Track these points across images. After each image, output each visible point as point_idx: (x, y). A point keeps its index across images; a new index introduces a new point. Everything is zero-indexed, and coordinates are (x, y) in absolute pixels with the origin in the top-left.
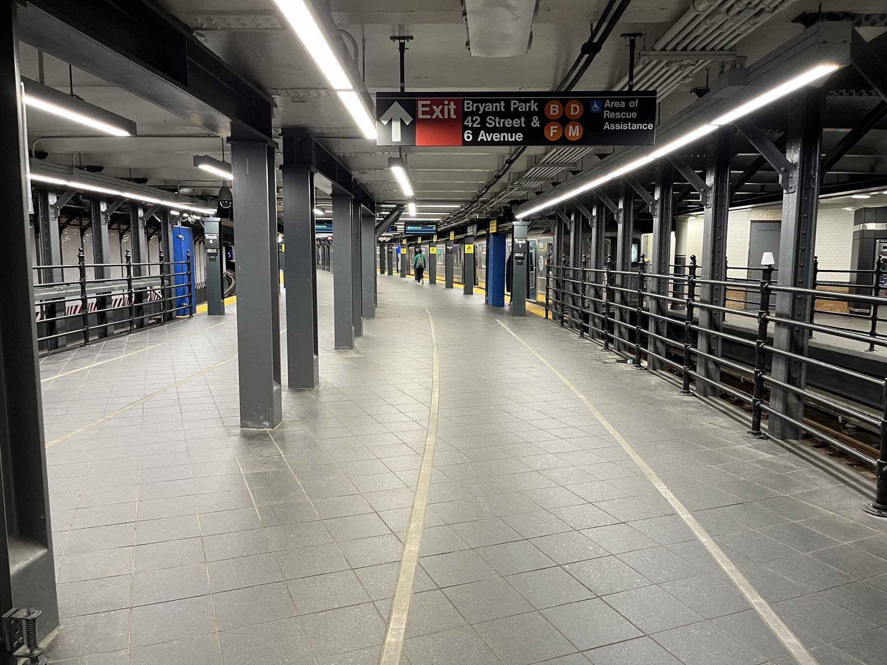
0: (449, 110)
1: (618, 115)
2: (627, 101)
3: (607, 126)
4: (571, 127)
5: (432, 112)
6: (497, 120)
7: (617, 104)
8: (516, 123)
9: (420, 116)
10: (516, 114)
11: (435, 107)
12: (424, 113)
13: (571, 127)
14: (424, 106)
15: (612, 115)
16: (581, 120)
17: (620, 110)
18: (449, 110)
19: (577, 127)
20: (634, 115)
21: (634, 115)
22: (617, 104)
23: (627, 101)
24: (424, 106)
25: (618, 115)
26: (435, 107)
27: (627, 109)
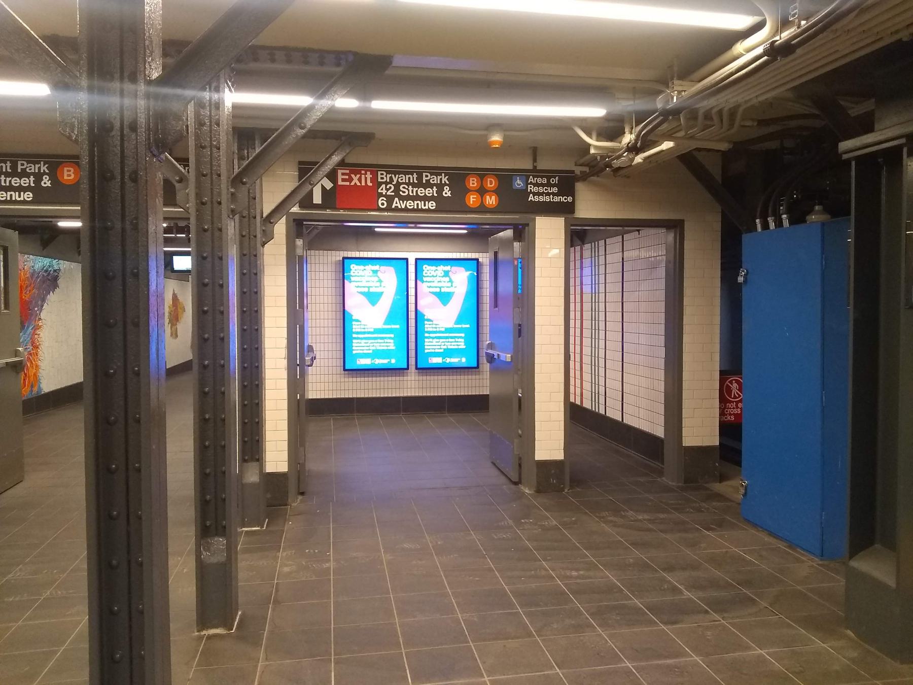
0: (366, 178)
1: (541, 190)
2: (549, 178)
3: (531, 198)
4: (488, 197)
5: (351, 180)
6: (410, 188)
7: (539, 180)
8: (429, 192)
9: (340, 183)
10: (428, 185)
11: (353, 176)
12: (343, 180)
13: (488, 197)
14: (343, 174)
15: (535, 189)
16: (496, 192)
17: (543, 185)
18: (366, 178)
19: (493, 197)
20: (555, 190)
21: (555, 190)
22: (539, 180)
23: (549, 178)
24: (343, 174)
25: (541, 190)
26: (353, 176)
27: (549, 185)
